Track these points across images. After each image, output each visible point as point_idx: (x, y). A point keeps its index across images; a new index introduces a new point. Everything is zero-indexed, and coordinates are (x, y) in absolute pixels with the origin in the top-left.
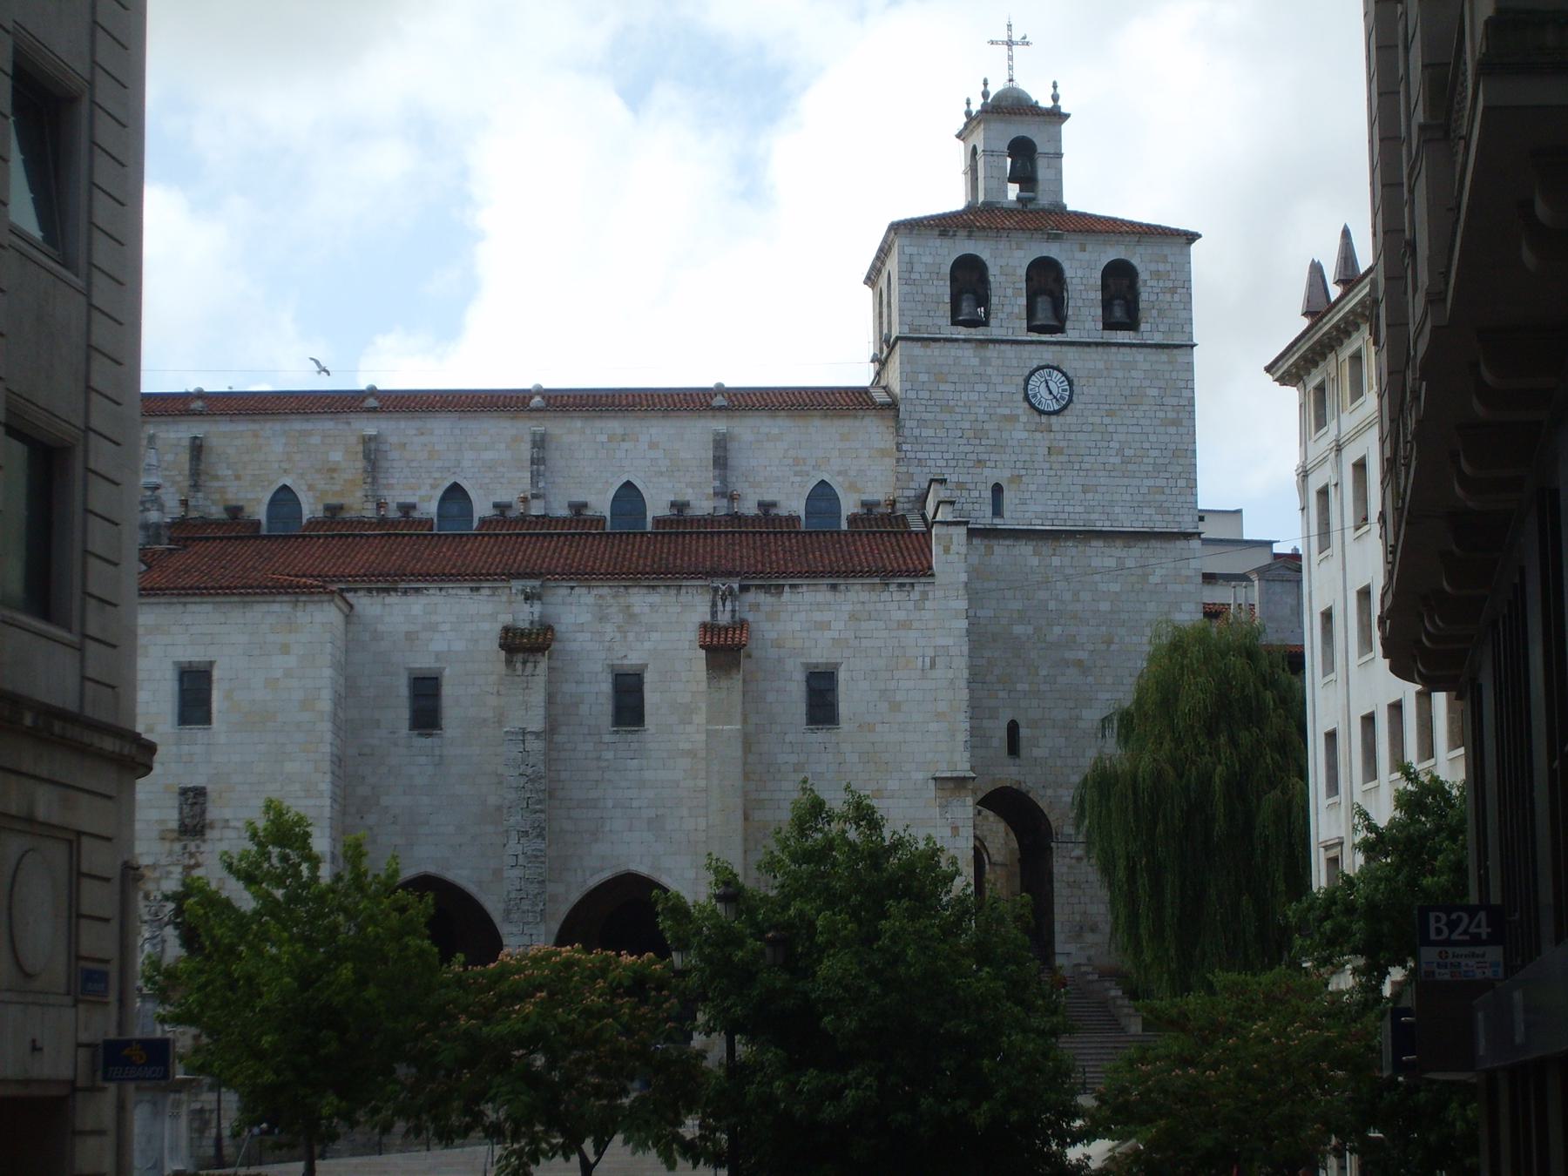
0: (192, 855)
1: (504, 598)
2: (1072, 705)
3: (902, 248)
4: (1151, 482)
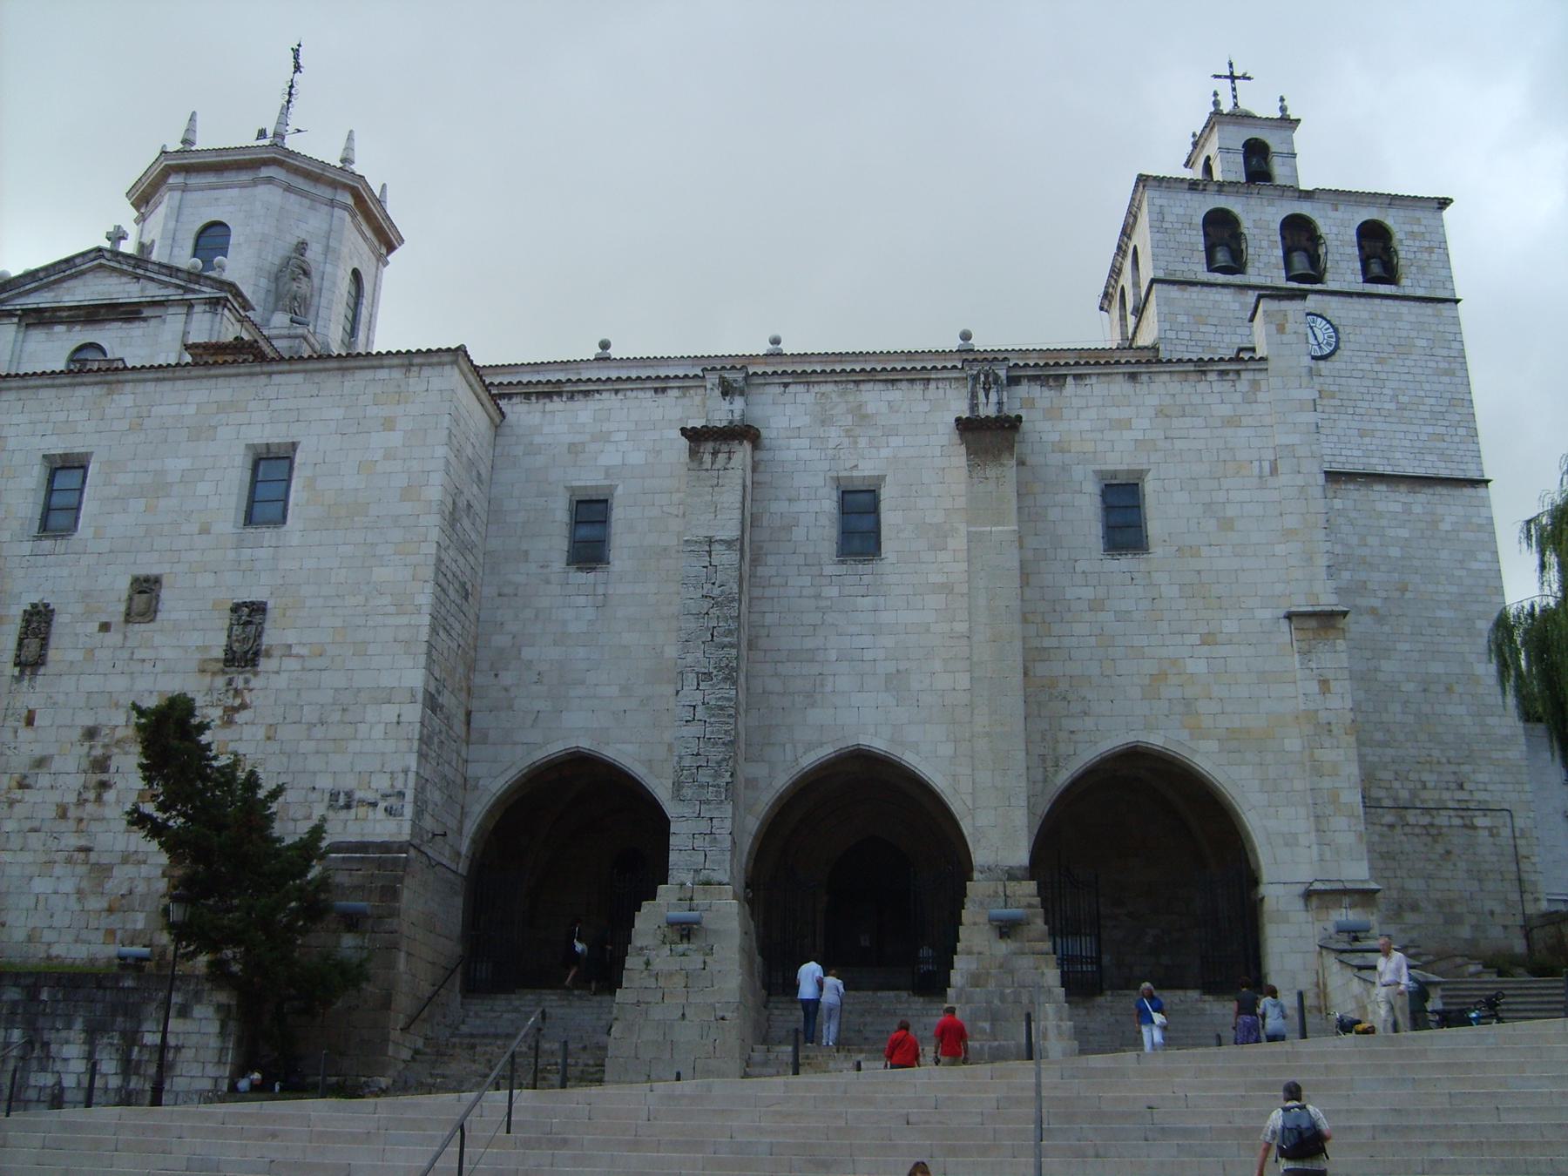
0: (237, 692)
1: (698, 400)
2: (1368, 654)
3: (1151, 204)
4: (1430, 429)
